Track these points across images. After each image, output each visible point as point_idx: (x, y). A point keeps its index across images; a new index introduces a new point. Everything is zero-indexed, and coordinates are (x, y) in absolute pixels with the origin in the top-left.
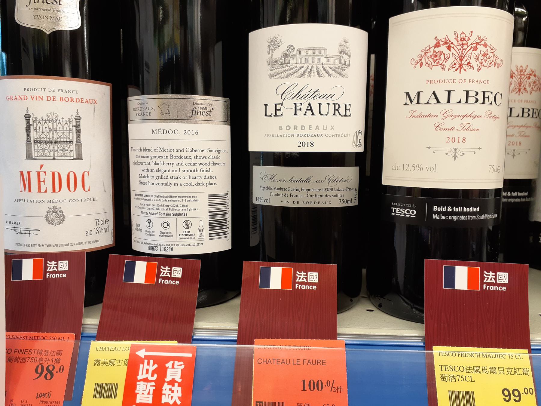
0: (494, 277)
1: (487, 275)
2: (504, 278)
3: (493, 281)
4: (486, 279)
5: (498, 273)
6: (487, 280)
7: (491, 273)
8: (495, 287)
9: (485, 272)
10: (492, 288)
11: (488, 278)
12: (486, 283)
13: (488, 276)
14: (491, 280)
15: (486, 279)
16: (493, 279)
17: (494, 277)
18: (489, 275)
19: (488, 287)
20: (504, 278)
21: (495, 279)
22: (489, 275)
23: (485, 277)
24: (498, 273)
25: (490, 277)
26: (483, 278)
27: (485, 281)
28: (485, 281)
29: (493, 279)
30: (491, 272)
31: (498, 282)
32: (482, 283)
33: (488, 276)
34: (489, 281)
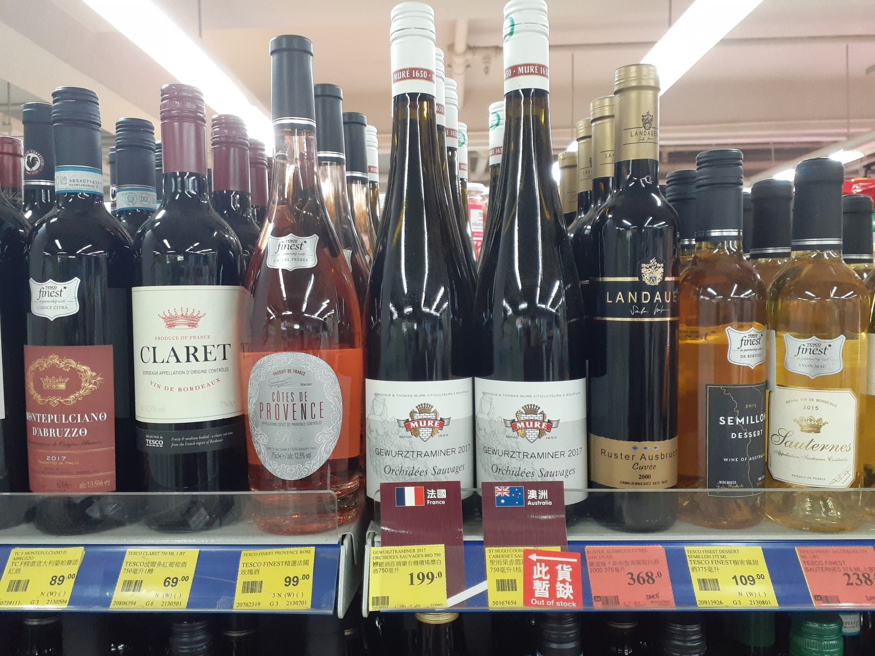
0: (435, 494)
1: (430, 492)
2: (443, 494)
3: (435, 497)
5: (438, 490)
7: (432, 491)
9: (428, 490)
10: (434, 503)
11: (430, 495)
12: (429, 499)
14: (433, 496)
17: (435, 494)
18: (431, 492)
19: (431, 502)
20: (443, 494)
21: (436, 495)
22: (431, 492)
23: (428, 494)
24: (438, 490)
25: (432, 494)
26: (426, 495)
28: (428, 498)
31: (438, 497)
32: (426, 499)
34: (431, 497)
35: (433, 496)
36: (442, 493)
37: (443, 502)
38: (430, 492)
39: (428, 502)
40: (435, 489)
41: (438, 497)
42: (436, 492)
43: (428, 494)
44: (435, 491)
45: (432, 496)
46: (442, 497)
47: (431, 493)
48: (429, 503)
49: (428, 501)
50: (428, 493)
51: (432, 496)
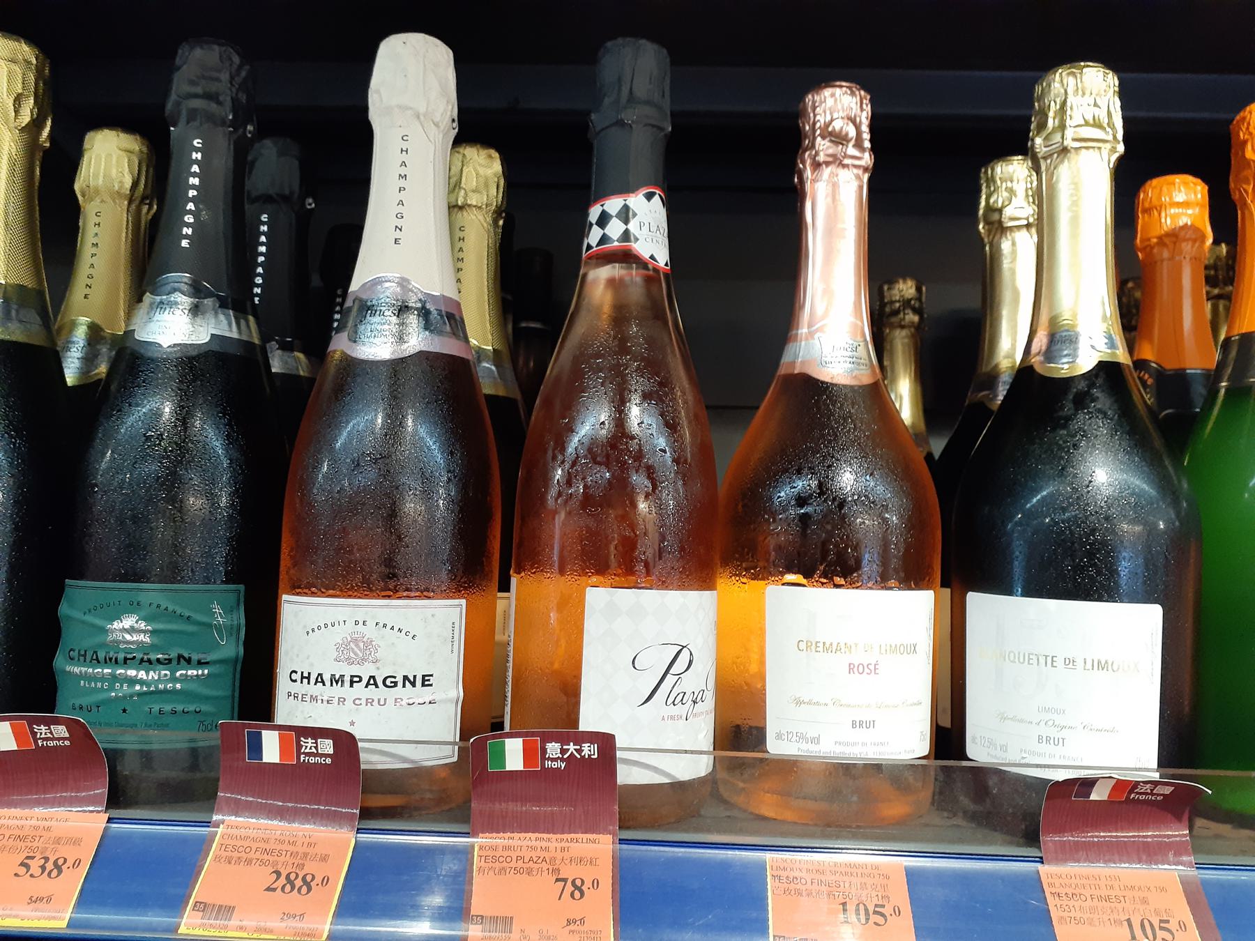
0: (315, 745)
1: (305, 742)
4: (304, 747)
5: (319, 740)
6: (305, 749)
7: (310, 740)
8: (316, 758)
9: (302, 739)
10: (312, 760)
11: (306, 747)
12: (304, 753)
13: (306, 745)
14: (311, 748)
15: (304, 747)
16: (313, 748)
17: (315, 745)
18: (308, 743)
19: (307, 758)
21: (316, 748)
22: (308, 743)
23: (302, 746)
24: (319, 740)
25: (309, 745)
26: (299, 747)
27: (302, 751)
28: (302, 751)
29: (313, 748)
30: (310, 739)
31: (320, 752)
33: (306, 745)
34: (307, 750)
35: (311, 748)
36: (327, 746)
37: (329, 761)
38: (305, 742)
39: (302, 759)
40: (315, 738)
41: (320, 752)
42: (316, 743)
43: (302, 746)
44: (314, 741)
45: (309, 748)
46: (326, 752)
47: (307, 745)
48: (304, 761)
49: (302, 756)
50: (302, 743)
51: (309, 748)
